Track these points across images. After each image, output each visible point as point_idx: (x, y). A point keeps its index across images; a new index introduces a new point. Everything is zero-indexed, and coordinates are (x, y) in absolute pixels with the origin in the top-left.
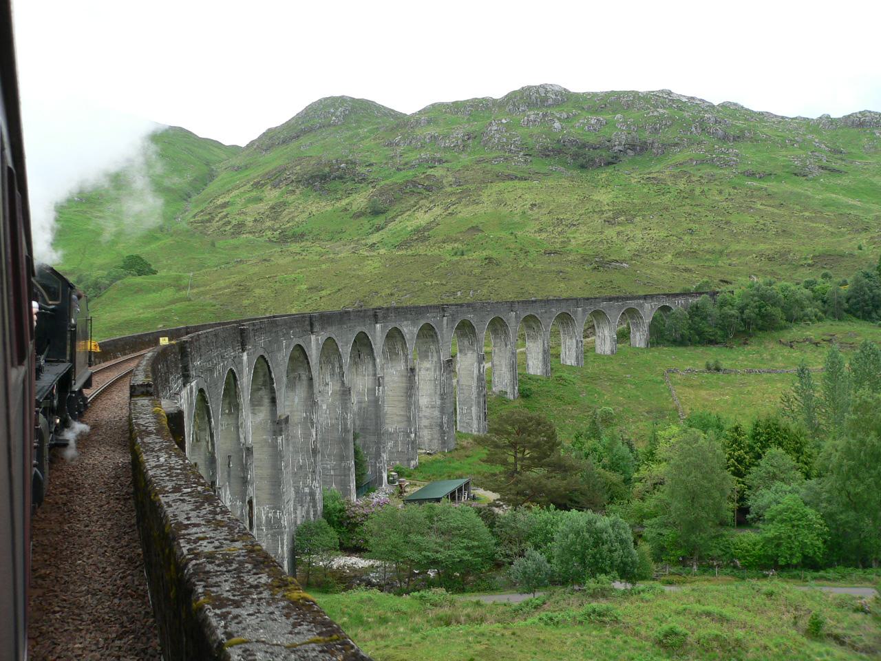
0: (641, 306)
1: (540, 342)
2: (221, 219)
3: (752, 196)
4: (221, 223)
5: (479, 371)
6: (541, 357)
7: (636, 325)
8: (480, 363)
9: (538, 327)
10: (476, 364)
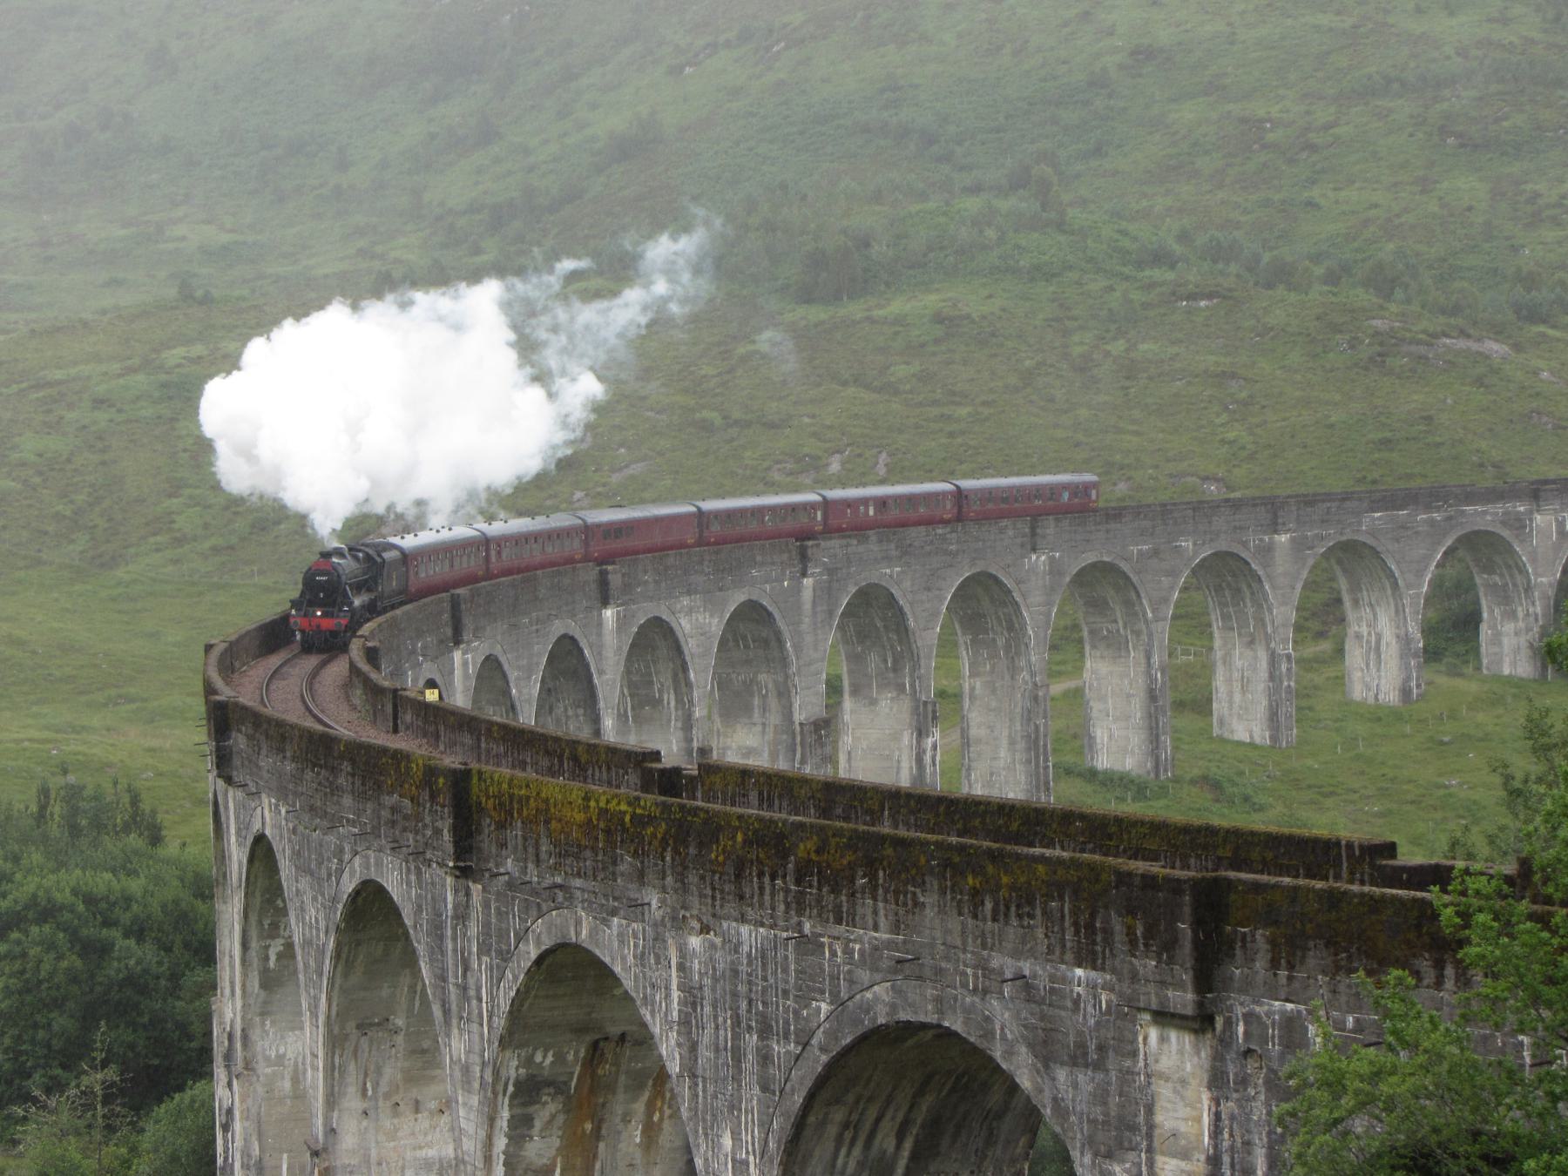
0: (1519, 524)
1: (1135, 655)
5: (920, 760)
6: (1137, 709)
7: (1504, 597)
8: (921, 733)
9: (1128, 604)
10: (907, 738)
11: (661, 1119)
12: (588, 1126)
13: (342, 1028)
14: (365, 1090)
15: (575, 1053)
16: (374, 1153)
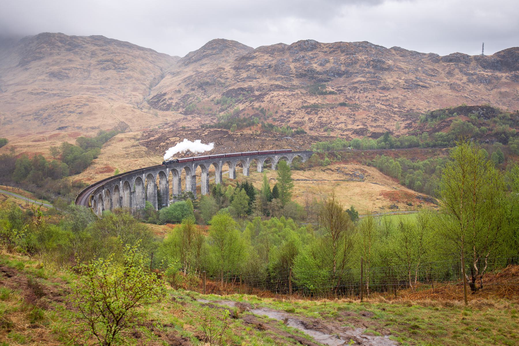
3: (379, 100)
4: (162, 103)
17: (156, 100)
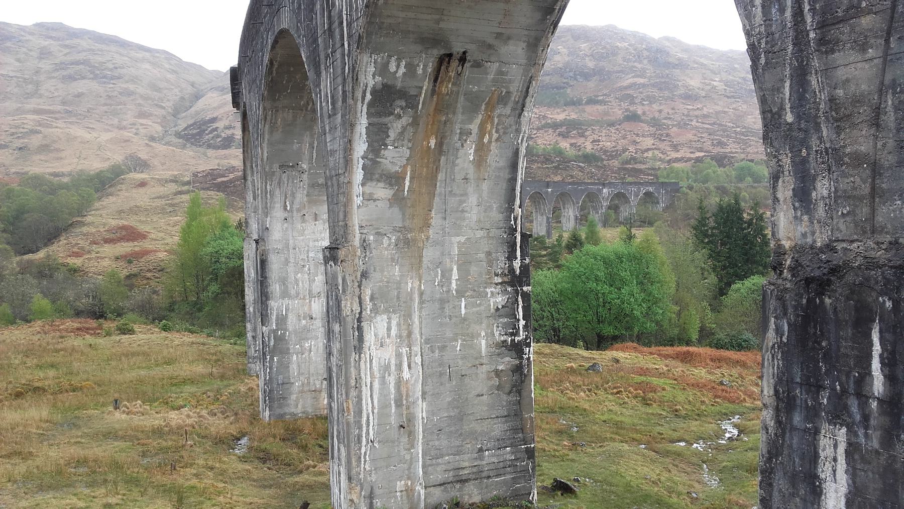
0: (600, 191)
2: (211, 132)
11: (490, 142)
12: (433, 143)
13: (271, 168)
14: (285, 206)
15: (425, 66)
16: (291, 242)
17: (195, 132)
